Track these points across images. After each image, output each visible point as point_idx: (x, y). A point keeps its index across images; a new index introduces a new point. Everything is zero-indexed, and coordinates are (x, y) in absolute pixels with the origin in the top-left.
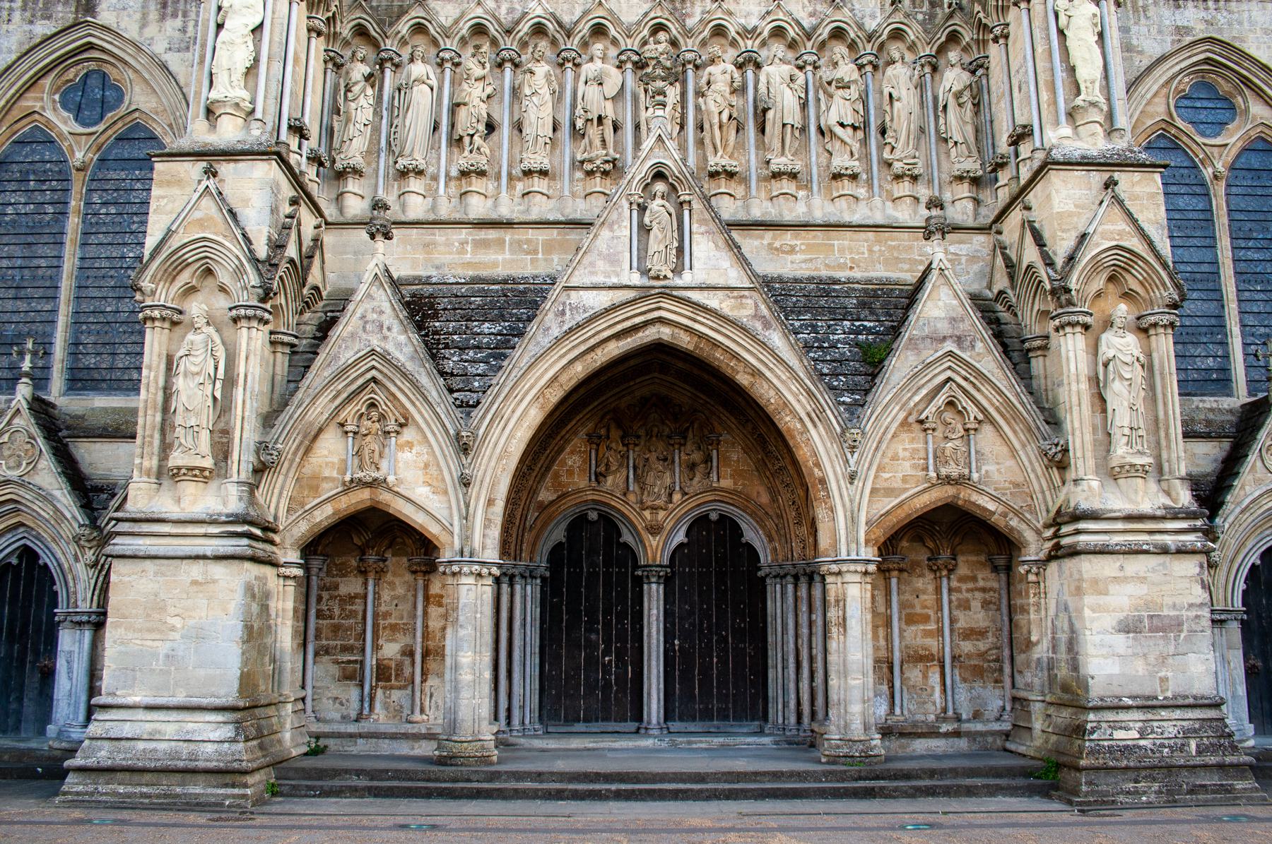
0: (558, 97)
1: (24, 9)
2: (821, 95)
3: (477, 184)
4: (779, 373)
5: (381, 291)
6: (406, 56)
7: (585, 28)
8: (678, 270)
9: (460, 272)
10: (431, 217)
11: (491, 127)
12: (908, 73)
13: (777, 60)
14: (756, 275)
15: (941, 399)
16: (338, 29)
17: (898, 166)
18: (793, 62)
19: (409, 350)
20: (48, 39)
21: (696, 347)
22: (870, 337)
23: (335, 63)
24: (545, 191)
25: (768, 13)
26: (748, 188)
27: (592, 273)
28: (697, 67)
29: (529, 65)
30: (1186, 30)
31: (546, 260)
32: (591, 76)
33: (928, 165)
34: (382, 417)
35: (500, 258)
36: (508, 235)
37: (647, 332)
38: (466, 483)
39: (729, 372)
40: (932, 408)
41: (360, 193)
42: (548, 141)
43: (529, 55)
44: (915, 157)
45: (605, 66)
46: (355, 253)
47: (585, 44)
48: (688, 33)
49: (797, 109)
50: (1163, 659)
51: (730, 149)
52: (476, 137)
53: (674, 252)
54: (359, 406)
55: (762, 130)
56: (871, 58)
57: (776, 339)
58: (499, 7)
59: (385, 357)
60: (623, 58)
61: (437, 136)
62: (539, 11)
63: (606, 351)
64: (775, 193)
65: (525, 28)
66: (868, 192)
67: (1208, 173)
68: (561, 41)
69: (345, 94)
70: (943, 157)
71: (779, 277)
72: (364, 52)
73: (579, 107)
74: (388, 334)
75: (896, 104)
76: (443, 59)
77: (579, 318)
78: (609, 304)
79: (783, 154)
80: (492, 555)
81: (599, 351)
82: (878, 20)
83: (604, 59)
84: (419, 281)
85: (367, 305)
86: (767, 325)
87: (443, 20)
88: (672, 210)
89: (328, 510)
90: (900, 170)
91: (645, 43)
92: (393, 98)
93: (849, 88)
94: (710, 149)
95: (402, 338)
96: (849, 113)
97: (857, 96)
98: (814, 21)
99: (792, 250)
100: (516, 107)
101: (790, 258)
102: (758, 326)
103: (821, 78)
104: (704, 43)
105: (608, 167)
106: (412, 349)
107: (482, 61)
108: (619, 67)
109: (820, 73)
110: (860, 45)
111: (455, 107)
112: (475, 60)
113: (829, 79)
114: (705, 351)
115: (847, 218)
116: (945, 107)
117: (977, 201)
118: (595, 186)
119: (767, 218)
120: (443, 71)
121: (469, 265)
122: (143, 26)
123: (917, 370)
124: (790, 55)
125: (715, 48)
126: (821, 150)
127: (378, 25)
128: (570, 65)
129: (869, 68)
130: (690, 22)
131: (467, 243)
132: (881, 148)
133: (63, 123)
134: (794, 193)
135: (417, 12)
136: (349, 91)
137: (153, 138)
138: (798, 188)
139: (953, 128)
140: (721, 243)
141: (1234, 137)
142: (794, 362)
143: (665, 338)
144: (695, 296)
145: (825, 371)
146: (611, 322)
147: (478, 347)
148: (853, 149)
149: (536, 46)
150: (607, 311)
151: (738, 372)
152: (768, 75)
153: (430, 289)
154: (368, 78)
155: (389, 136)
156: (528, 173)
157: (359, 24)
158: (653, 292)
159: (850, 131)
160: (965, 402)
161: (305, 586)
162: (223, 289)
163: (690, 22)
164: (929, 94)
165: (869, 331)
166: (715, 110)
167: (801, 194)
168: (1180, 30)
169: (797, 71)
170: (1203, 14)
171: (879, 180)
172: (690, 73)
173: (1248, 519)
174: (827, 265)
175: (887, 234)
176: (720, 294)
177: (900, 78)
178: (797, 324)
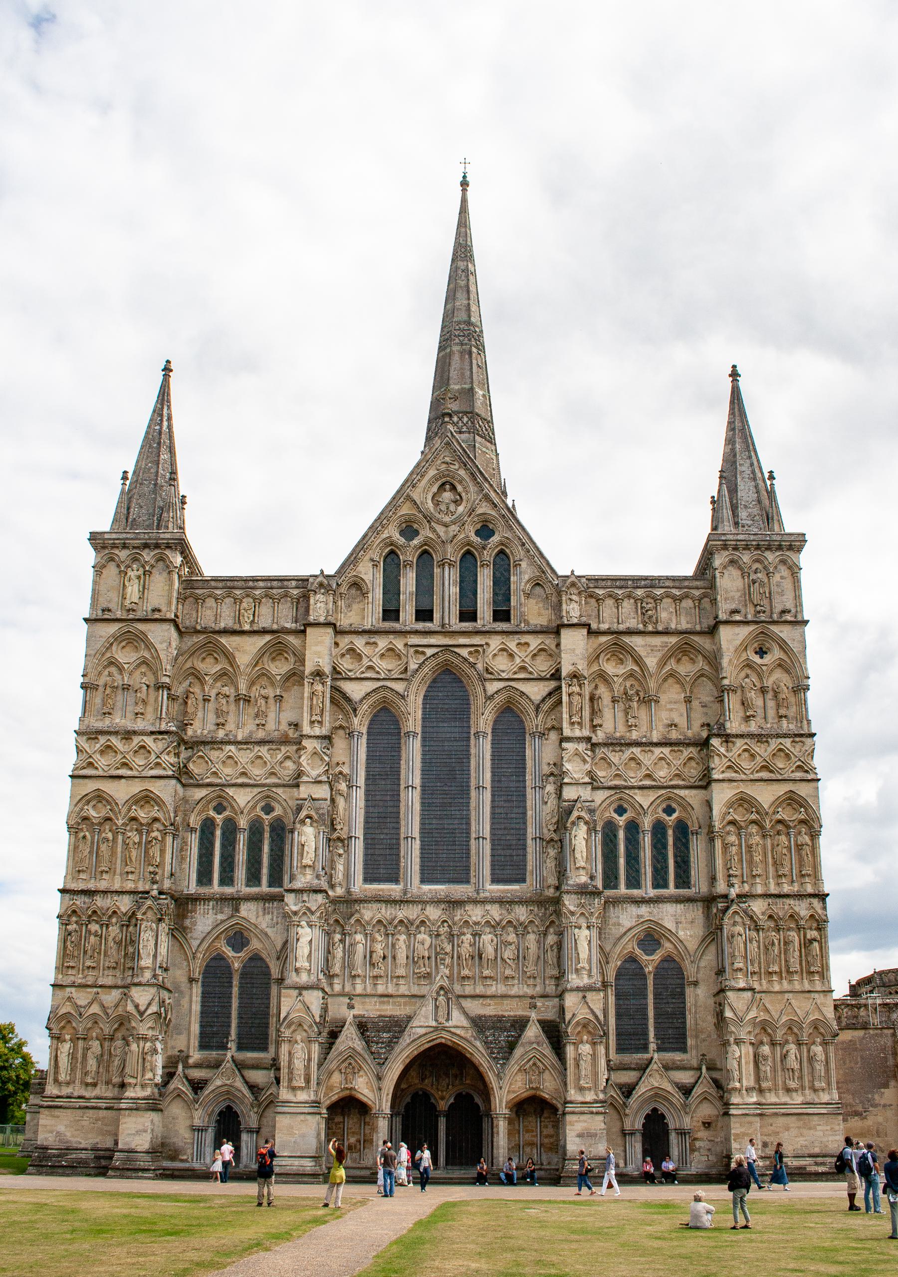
0: (408, 947)
1: (213, 909)
6: (354, 930)
7: (417, 922)
8: (447, 1020)
10: (364, 993)
11: (384, 958)
15: (531, 1063)
20: (222, 921)
23: (328, 934)
30: (642, 916)
34: (353, 1068)
38: (380, 1089)
40: (527, 1066)
48: (454, 924)
50: (590, 1145)
54: (345, 1064)
57: (478, 1044)
65: (396, 921)
67: (647, 970)
80: (388, 1111)
86: (475, 1039)
89: (336, 1097)
99: (490, 1005)
111: (371, 952)
114: (456, 1046)
117: (557, 985)
121: (377, 1010)
122: (257, 917)
125: (465, 930)
130: (456, 919)
132: (523, 965)
133: (229, 952)
137: (261, 959)
141: (657, 957)
142: (483, 1052)
144: (453, 1030)
147: (382, 1043)
150: (424, 1035)
154: (341, 941)
156: (398, 977)
160: (539, 1064)
161: (329, 1121)
162: (305, 1030)
165: (512, 1036)
168: (639, 916)
170: (648, 909)
173: (641, 1099)
177: (532, 937)
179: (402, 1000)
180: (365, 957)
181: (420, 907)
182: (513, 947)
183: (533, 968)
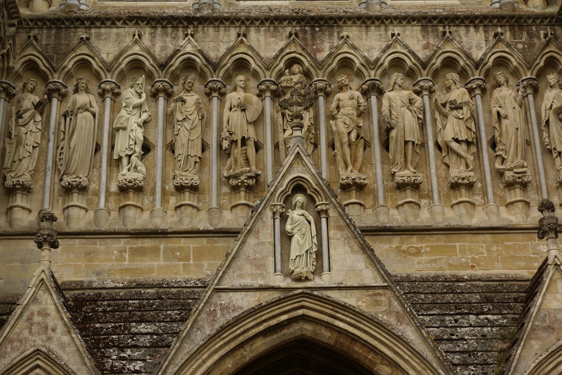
0: (205, 121)
2: (437, 116)
3: (132, 200)
4: (415, 364)
5: (47, 296)
6: (71, 89)
7: (229, 63)
8: (318, 271)
9: (118, 277)
10: (93, 228)
11: (147, 148)
12: (513, 94)
13: (397, 87)
14: (389, 275)
16: (11, 64)
17: (509, 175)
18: (411, 87)
19: (71, 349)
21: (337, 342)
22: (494, 329)
24: (195, 204)
25: (389, 47)
26: (376, 198)
27: (241, 276)
28: (327, 95)
29: (181, 94)
31: (196, 266)
32: (235, 103)
33: (536, 173)
35: (155, 264)
36: (162, 244)
37: (291, 330)
39: (367, 363)
41: (28, 206)
42: (198, 160)
43: (180, 87)
44: (523, 167)
45: (248, 94)
46: (22, 261)
47: (229, 77)
49: (417, 128)
51: (359, 164)
52: (133, 157)
53: (314, 256)
55: (386, 146)
56: (480, 82)
58: (154, 45)
59: (48, 357)
60: (263, 87)
61: (98, 156)
62: (189, 49)
63: (254, 347)
64: (400, 202)
65: (177, 63)
66: (483, 198)
68: (208, 73)
69: (16, 120)
70: (548, 166)
71: (408, 276)
72: (34, 84)
73: (225, 130)
74: (52, 335)
75: (504, 122)
76: (104, 91)
77: (231, 316)
78: (257, 303)
79: (406, 167)
81: (248, 348)
82: (484, 50)
83: (245, 89)
84: (80, 286)
85: (34, 308)
87: (104, 56)
88: (311, 218)
90: (511, 179)
91: (281, 74)
92: (60, 124)
93: (462, 108)
94: (341, 164)
95: (66, 339)
96: (462, 130)
97: (469, 115)
98: (428, 53)
99: (418, 252)
100: (169, 131)
101: (416, 259)
102: (392, 320)
103: (436, 100)
104: (332, 74)
105: (251, 182)
106: (74, 349)
107: (139, 91)
108: (259, 96)
109: (436, 96)
110: (470, 72)
111: (114, 132)
112: (132, 90)
113: (443, 102)
115: (466, 222)
116: (547, 122)
118: (240, 199)
119: (395, 224)
120: (104, 101)
121: (127, 270)
123: (541, 358)
124: (408, 83)
125: (342, 78)
126: (439, 163)
127: (47, 60)
128: (216, 94)
129: (478, 92)
131: (125, 251)
134: (418, 202)
135: (84, 50)
136: (21, 117)
138: (421, 197)
139: (556, 140)
140: (356, 248)
143: (309, 334)
144: (335, 295)
145: (456, 361)
146: (258, 321)
148: (468, 161)
149: (186, 78)
151: (375, 364)
152: (389, 99)
153: (92, 293)
155: (54, 158)
156: (180, 189)
157: (30, 60)
158: (296, 292)
159: (464, 146)
163: (321, 56)
164: (533, 111)
165: (492, 324)
166: (344, 130)
167: (423, 202)
169: (415, 96)
171: (493, 187)
172: (321, 99)
174: (450, 265)
175: (503, 236)
176: (357, 293)
178: (427, 319)
179: (191, 244)
180: (98, 148)
181: (233, 32)
182: (465, 112)
183: (519, 161)
